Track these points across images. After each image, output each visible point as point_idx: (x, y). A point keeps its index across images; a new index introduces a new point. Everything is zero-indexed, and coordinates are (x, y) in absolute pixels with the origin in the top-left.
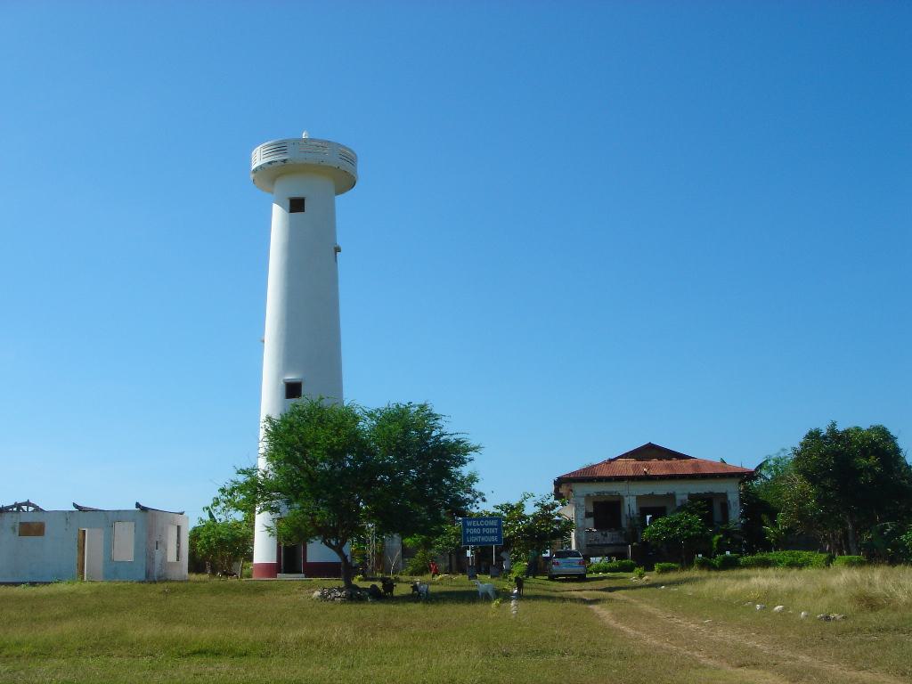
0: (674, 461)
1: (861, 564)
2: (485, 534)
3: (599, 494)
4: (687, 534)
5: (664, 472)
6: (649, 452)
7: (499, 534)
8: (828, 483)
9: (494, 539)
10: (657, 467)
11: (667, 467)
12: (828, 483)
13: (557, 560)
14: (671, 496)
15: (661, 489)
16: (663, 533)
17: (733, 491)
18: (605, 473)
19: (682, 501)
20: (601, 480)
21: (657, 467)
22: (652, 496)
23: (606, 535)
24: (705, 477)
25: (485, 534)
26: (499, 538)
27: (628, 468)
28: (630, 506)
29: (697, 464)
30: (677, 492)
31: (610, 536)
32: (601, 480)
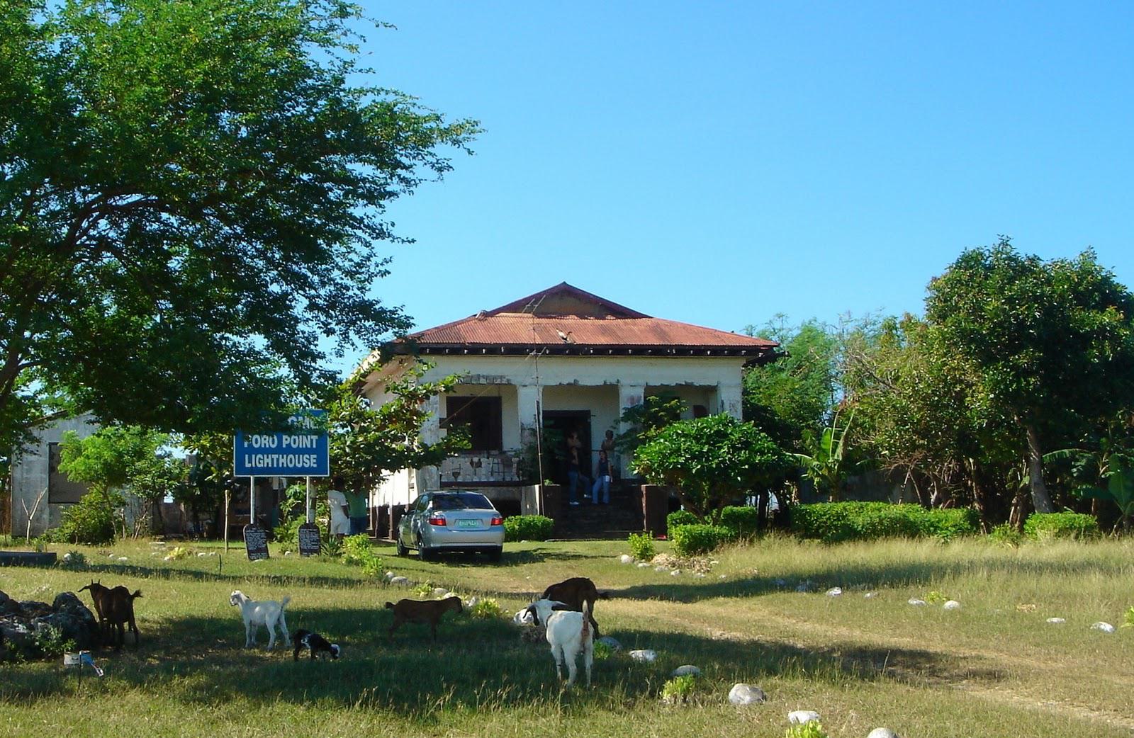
0: (610, 321)
1: (1087, 533)
2: (289, 450)
3: (468, 381)
4: (746, 462)
5: (603, 340)
6: (563, 300)
7: (320, 450)
8: (1022, 360)
9: (310, 461)
10: (586, 331)
11: (604, 331)
12: (1022, 360)
13: (437, 514)
14: (610, 391)
15: (592, 373)
16: (693, 457)
17: (729, 381)
18: (482, 335)
19: (632, 399)
20: (456, 350)
21: (586, 331)
22: (573, 389)
23: (479, 464)
24: (683, 352)
25: (289, 450)
26: (321, 461)
27: (524, 329)
28: (526, 410)
29: (657, 328)
30: (623, 382)
31: (487, 467)
32: (475, 350)
